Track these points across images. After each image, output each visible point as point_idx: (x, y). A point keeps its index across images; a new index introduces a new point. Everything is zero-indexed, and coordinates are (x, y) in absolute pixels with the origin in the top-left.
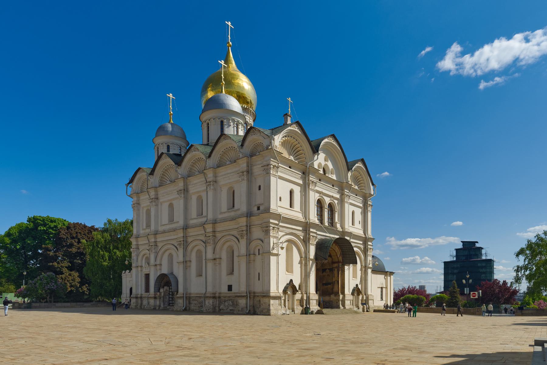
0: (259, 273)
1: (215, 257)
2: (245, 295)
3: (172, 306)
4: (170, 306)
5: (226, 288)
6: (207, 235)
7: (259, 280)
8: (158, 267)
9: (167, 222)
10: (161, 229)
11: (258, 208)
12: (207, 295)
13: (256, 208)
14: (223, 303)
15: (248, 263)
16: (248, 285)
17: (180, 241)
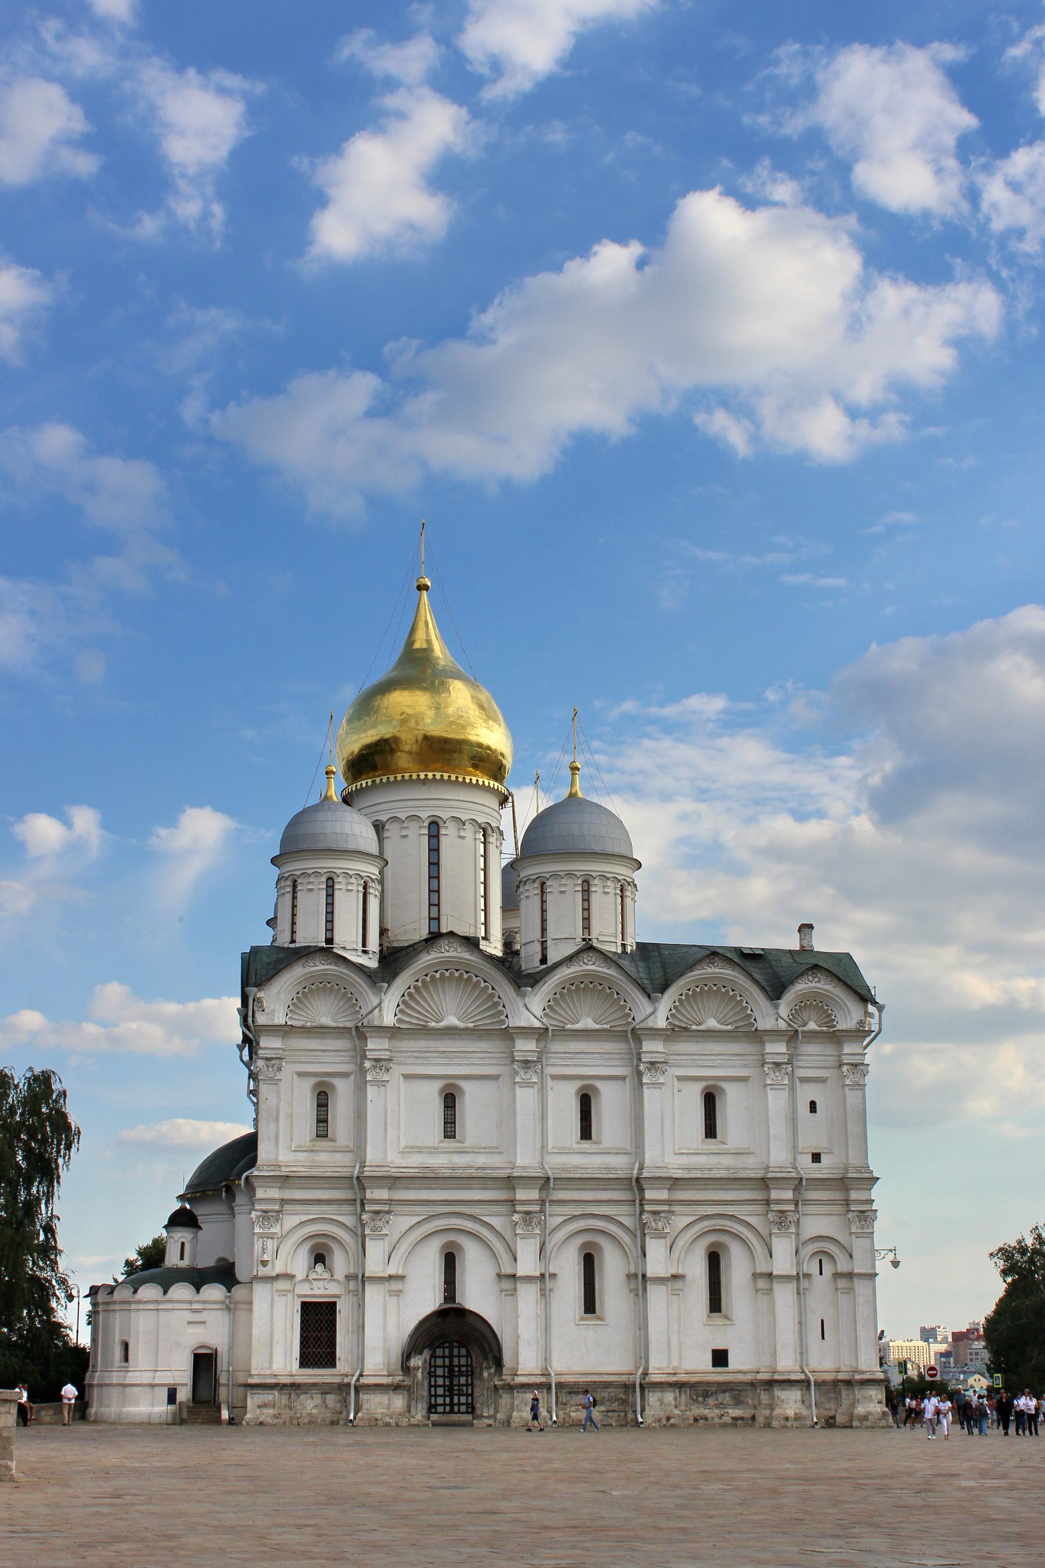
0: (822, 1321)
1: (674, 1271)
2: (802, 1377)
3: (444, 1412)
4: (436, 1413)
5: (709, 1357)
6: (647, 1208)
7: (823, 1338)
8: (395, 1286)
11: (816, 1157)
12: (655, 1378)
14: (700, 1399)
16: (803, 1351)
17: (528, 1213)
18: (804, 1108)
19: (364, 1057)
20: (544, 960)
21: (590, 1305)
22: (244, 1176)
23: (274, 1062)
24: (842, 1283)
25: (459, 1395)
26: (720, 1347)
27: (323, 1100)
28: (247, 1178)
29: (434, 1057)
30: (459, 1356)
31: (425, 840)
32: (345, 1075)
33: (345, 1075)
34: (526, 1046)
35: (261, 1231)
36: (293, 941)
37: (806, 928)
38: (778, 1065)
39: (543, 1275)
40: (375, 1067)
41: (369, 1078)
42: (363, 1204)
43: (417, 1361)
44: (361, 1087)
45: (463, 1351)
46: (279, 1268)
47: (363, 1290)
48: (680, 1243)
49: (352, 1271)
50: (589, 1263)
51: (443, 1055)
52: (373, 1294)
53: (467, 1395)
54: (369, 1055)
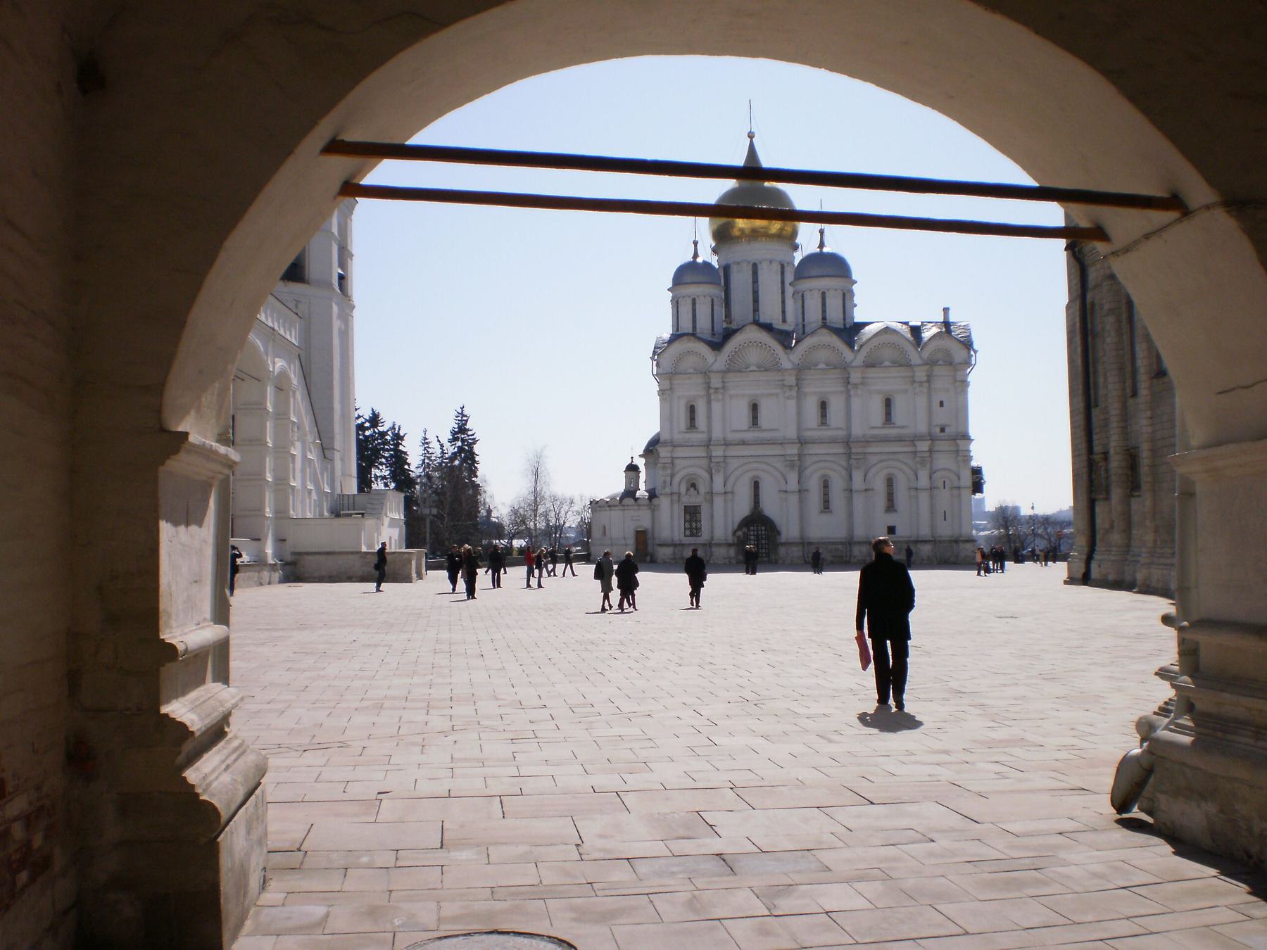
1: (867, 488)
6: (853, 457)
7: (945, 520)
8: (729, 496)
9: (746, 428)
10: (731, 437)
11: (943, 430)
12: (856, 540)
13: (938, 430)
15: (932, 497)
16: (933, 527)
18: (936, 405)
19: (709, 388)
20: (804, 333)
21: (826, 506)
24: (955, 492)
25: (762, 549)
26: (892, 525)
27: (692, 410)
30: (762, 530)
31: (751, 272)
36: (678, 330)
37: (946, 310)
38: (921, 382)
39: (800, 491)
40: (715, 392)
41: (712, 397)
42: (711, 459)
43: (740, 533)
44: (709, 402)
45: (763, 528)
46: (675, 489)
47: (712, 499)
48: (870, 474)
49: (707, 491)
50: (826, 485)
52: (719, 502)
53: (766, 549)
54: (712, 386)
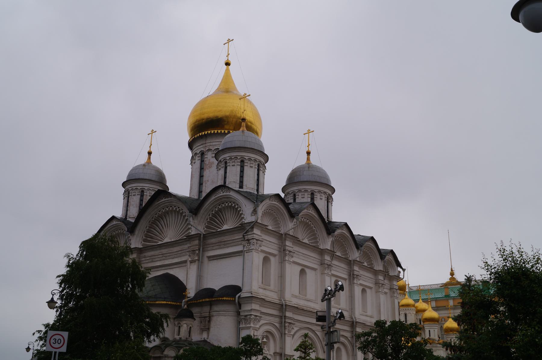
19: (284, 250)
22: (237, 296)
23: (259, 242)
28: (239, 297)
29: (301, 256)
32: (274, 255)
33: (274, 255)
34: (327, 258)
35: (254, 326)
51: (303, 255)
